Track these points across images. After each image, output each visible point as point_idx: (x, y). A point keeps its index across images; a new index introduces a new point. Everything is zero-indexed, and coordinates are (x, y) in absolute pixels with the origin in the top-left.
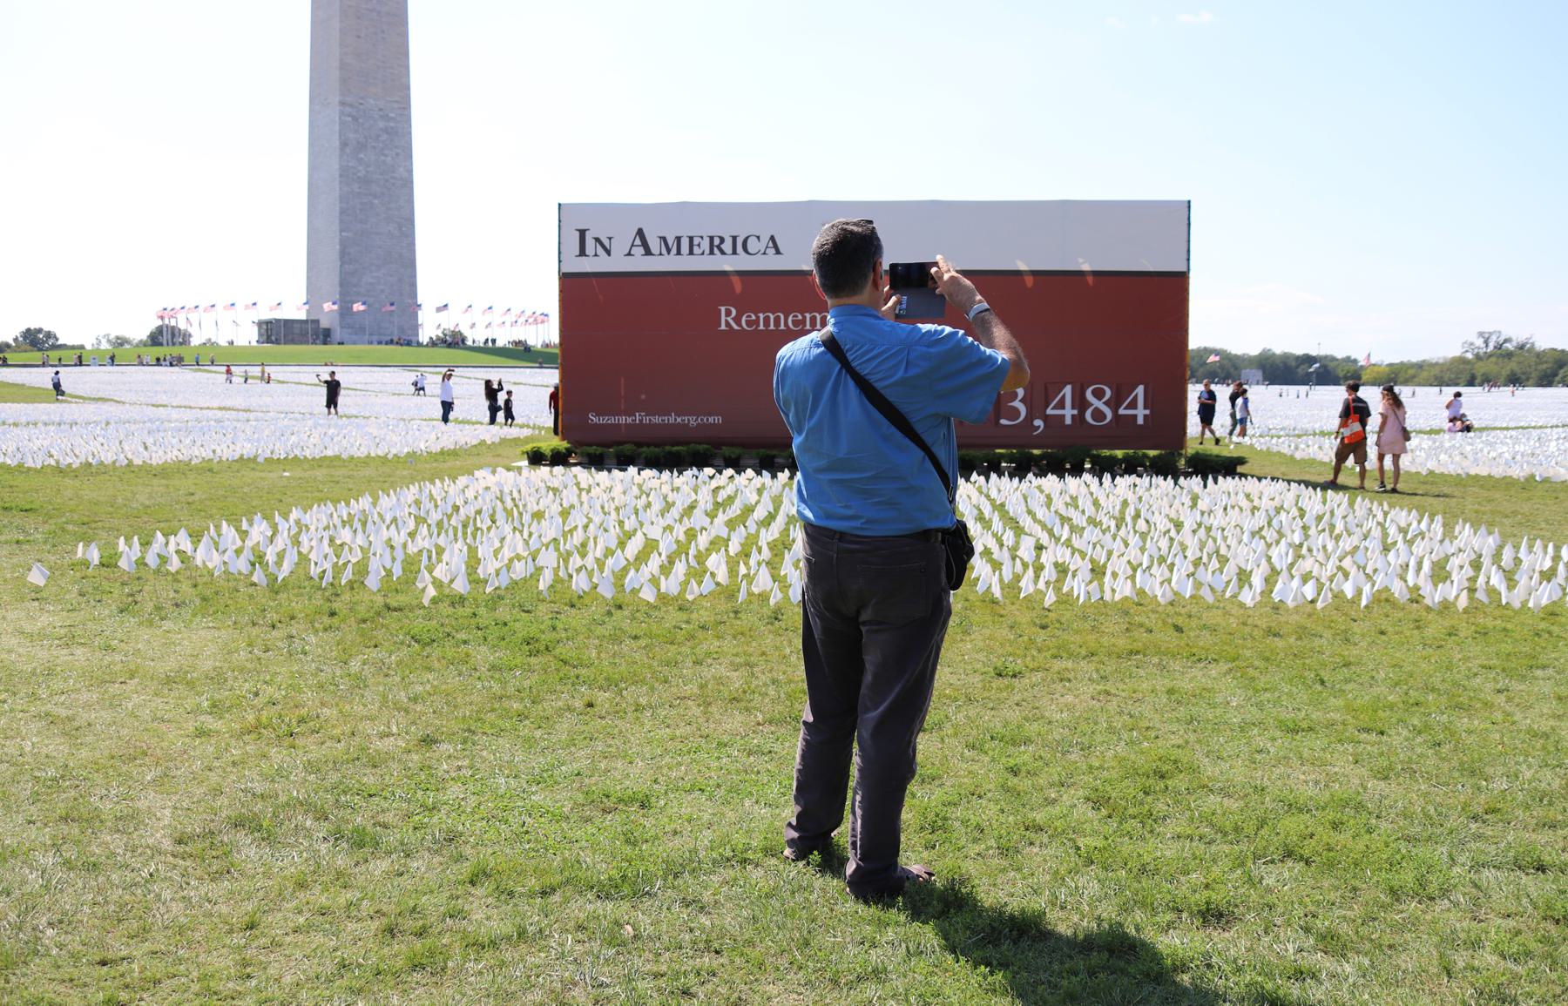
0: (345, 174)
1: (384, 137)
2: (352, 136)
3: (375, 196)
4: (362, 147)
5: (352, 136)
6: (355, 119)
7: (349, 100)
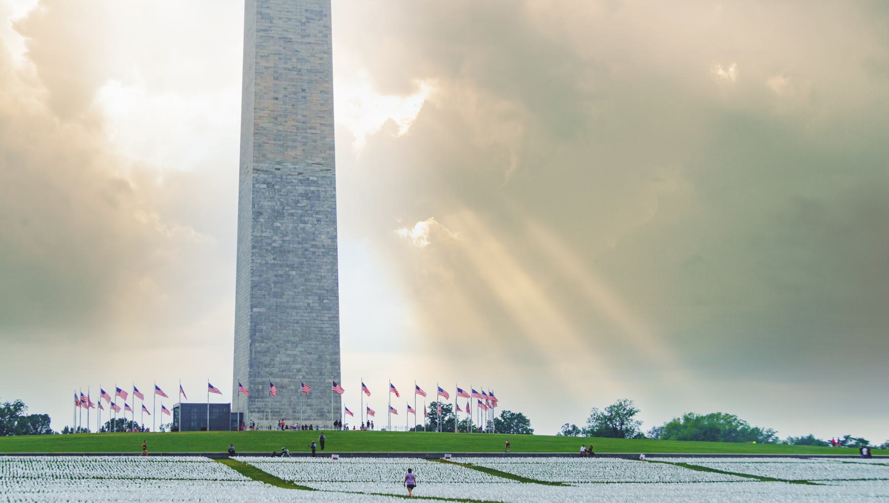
0: (258, 246)
1: (304, 202)
2: (266, 203)
3: (292, 267)
4: (278, 215)
5: (266, 204)
6: (270, 185)
7: (264, 166)
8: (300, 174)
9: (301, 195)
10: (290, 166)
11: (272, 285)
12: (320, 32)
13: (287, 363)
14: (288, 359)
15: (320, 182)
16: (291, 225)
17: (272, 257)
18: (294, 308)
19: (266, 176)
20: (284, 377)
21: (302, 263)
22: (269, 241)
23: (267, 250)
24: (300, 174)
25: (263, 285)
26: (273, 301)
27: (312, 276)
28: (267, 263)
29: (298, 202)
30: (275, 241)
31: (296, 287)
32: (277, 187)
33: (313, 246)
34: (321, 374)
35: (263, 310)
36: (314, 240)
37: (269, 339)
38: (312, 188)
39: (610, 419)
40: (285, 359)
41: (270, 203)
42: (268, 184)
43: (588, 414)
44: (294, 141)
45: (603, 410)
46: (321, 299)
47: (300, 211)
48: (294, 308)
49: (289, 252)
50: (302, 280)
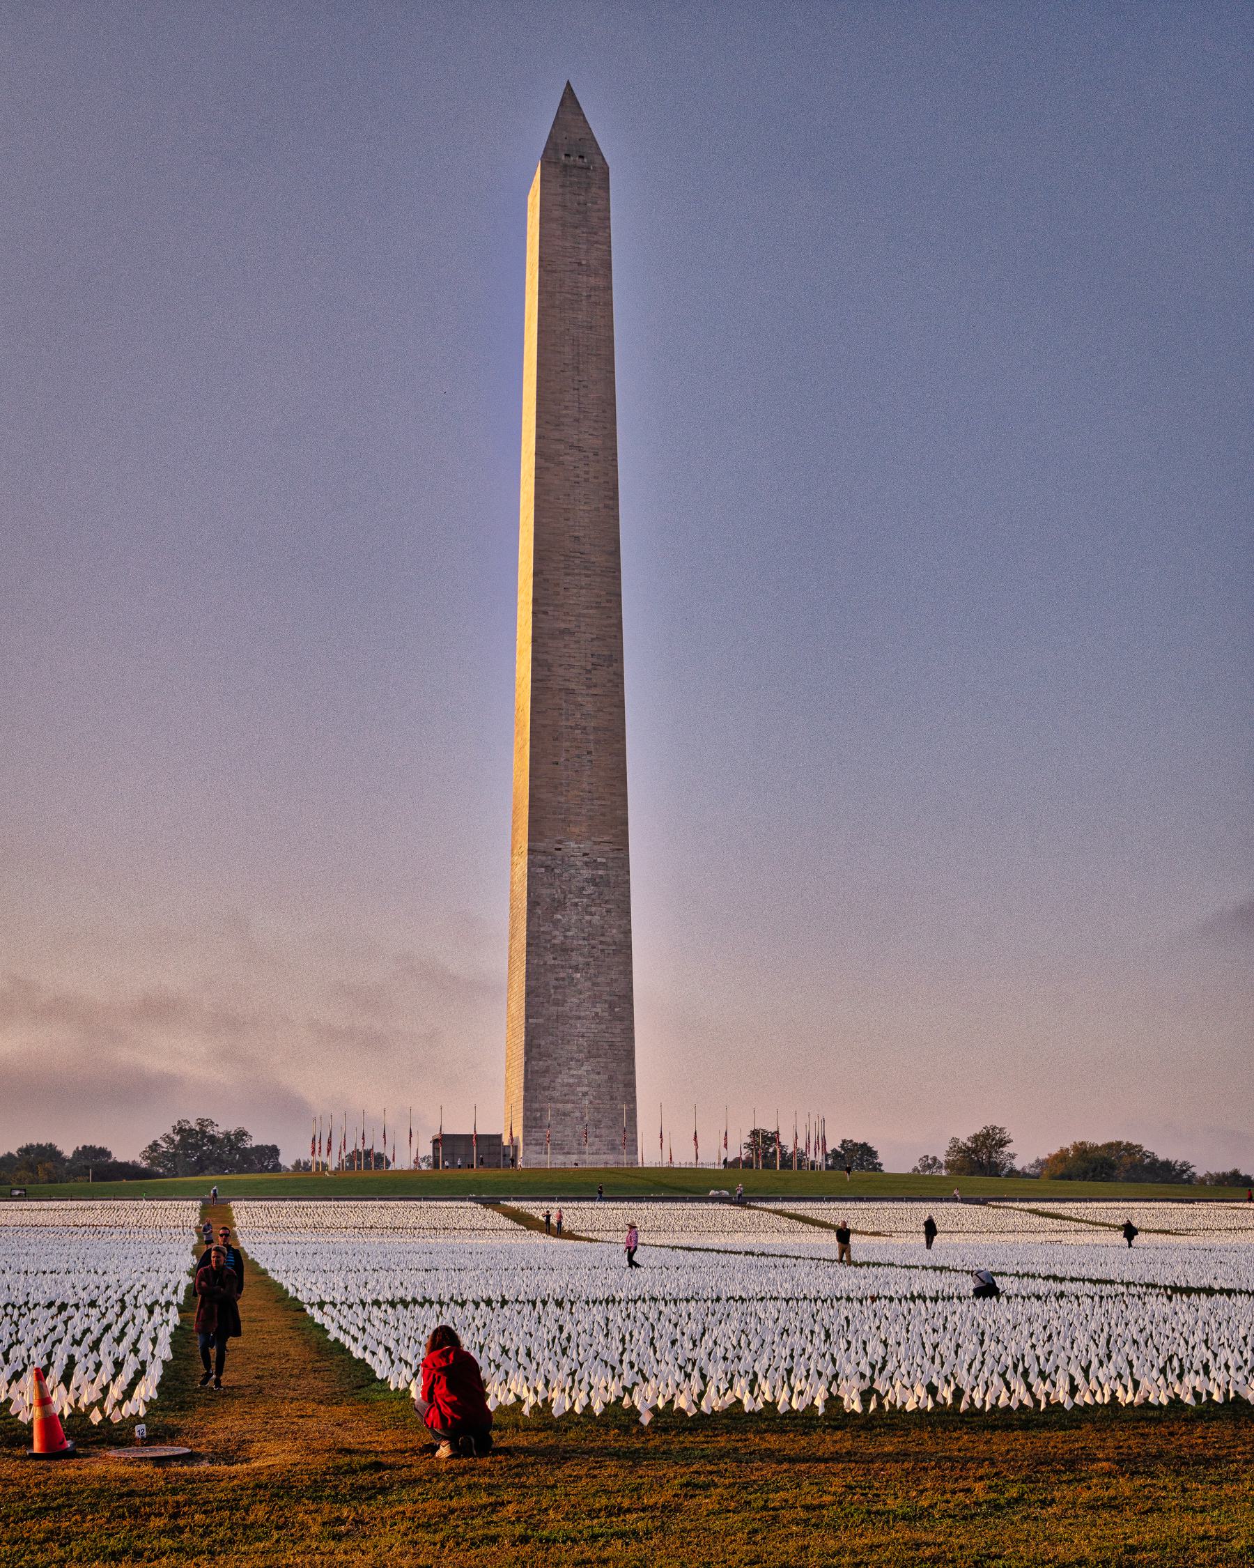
1: (590, 890)
3: (576, 969)
4: (559, 905)
8: (585, 854)
9: (587, 881)
10: (573, 845)
12: (610, 681)
13: (570, 1085)
14: (571, 1081)
15: (610, 864)
16: (575, 917)
18: (579, 1018)
19: (544, 858)
20: (567, 1102)
21: (588, 964)
22: (548, 937)
23: (545, 948)
24: (585, 854)
25: (541, 990)
26: (553, 1009)
27: (600, 979)
29: (583, 889)
30: (555, 937)
32: (557, 871)
33: (601, 943)
34: (612, 1098)
35: (541, 1021)
36: (603, 935)
37: (549, 1056)
38: (600, 872)
39: (975, 1151)
40: (566, 1081)
41: (548, 891)
42: (546, 867)
43: (946, 1146)
44: (578, 814)
45: (965, 1135)
47: (585, 900)
48: (579, 1018)
49: (572, 950)
50: (588, 984)
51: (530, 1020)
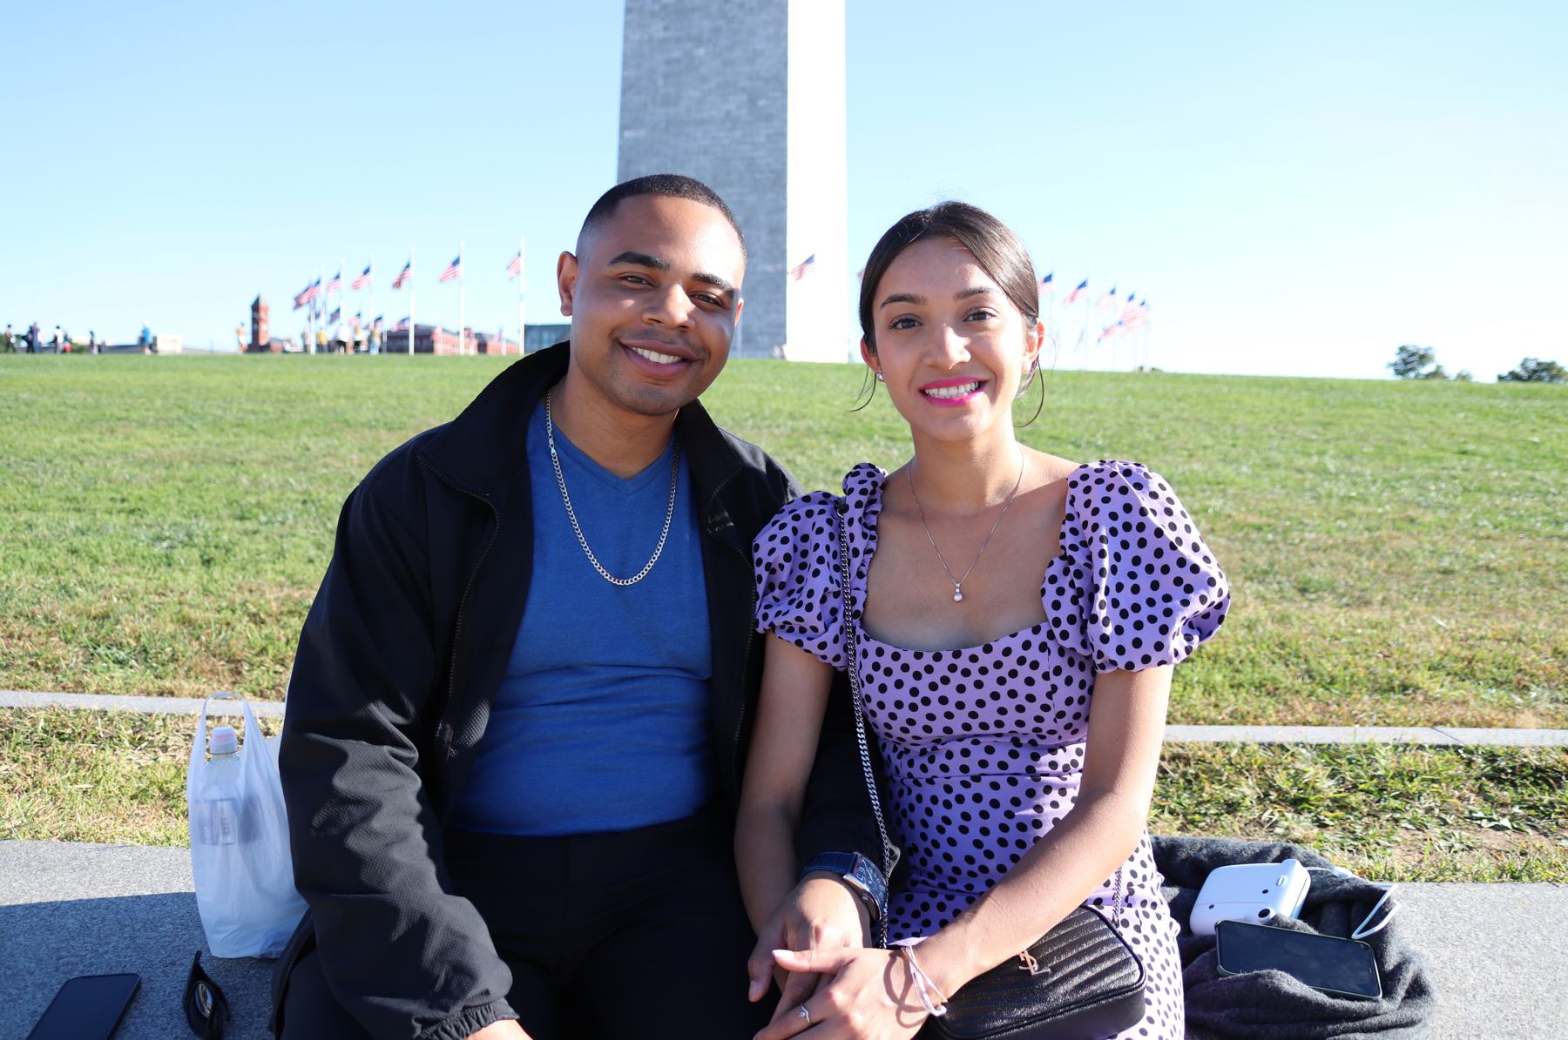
3: (699, 41)
11: (660, 82)
17: (661, 25)
21: (716, 31)
23: (653, 14)
28: (651, 39)
31: (704, 79)
35: (642, 133)
46: (752, 101)
49: (693, 10)
51: (627, 134)
